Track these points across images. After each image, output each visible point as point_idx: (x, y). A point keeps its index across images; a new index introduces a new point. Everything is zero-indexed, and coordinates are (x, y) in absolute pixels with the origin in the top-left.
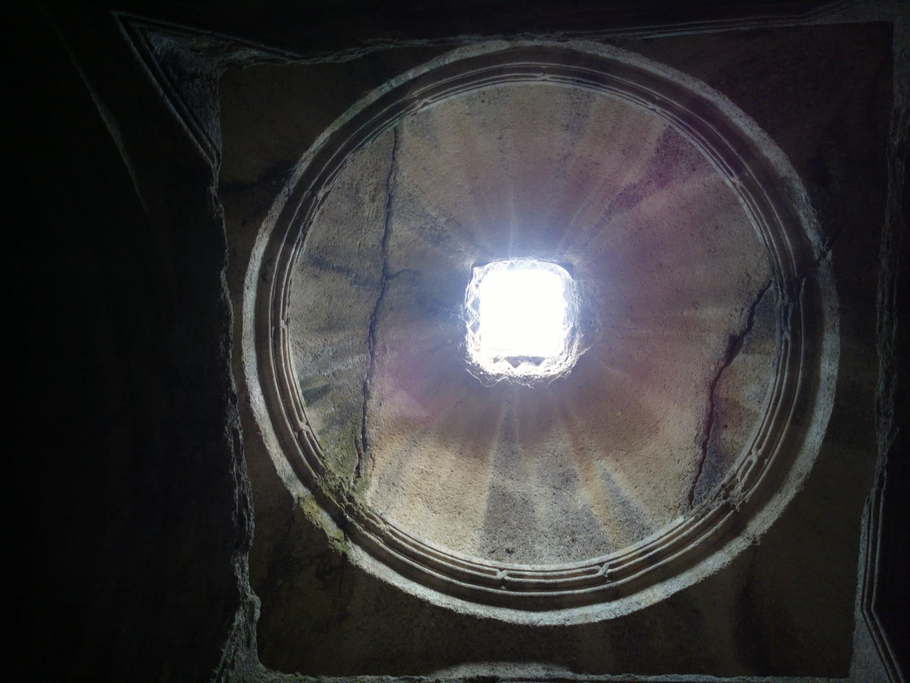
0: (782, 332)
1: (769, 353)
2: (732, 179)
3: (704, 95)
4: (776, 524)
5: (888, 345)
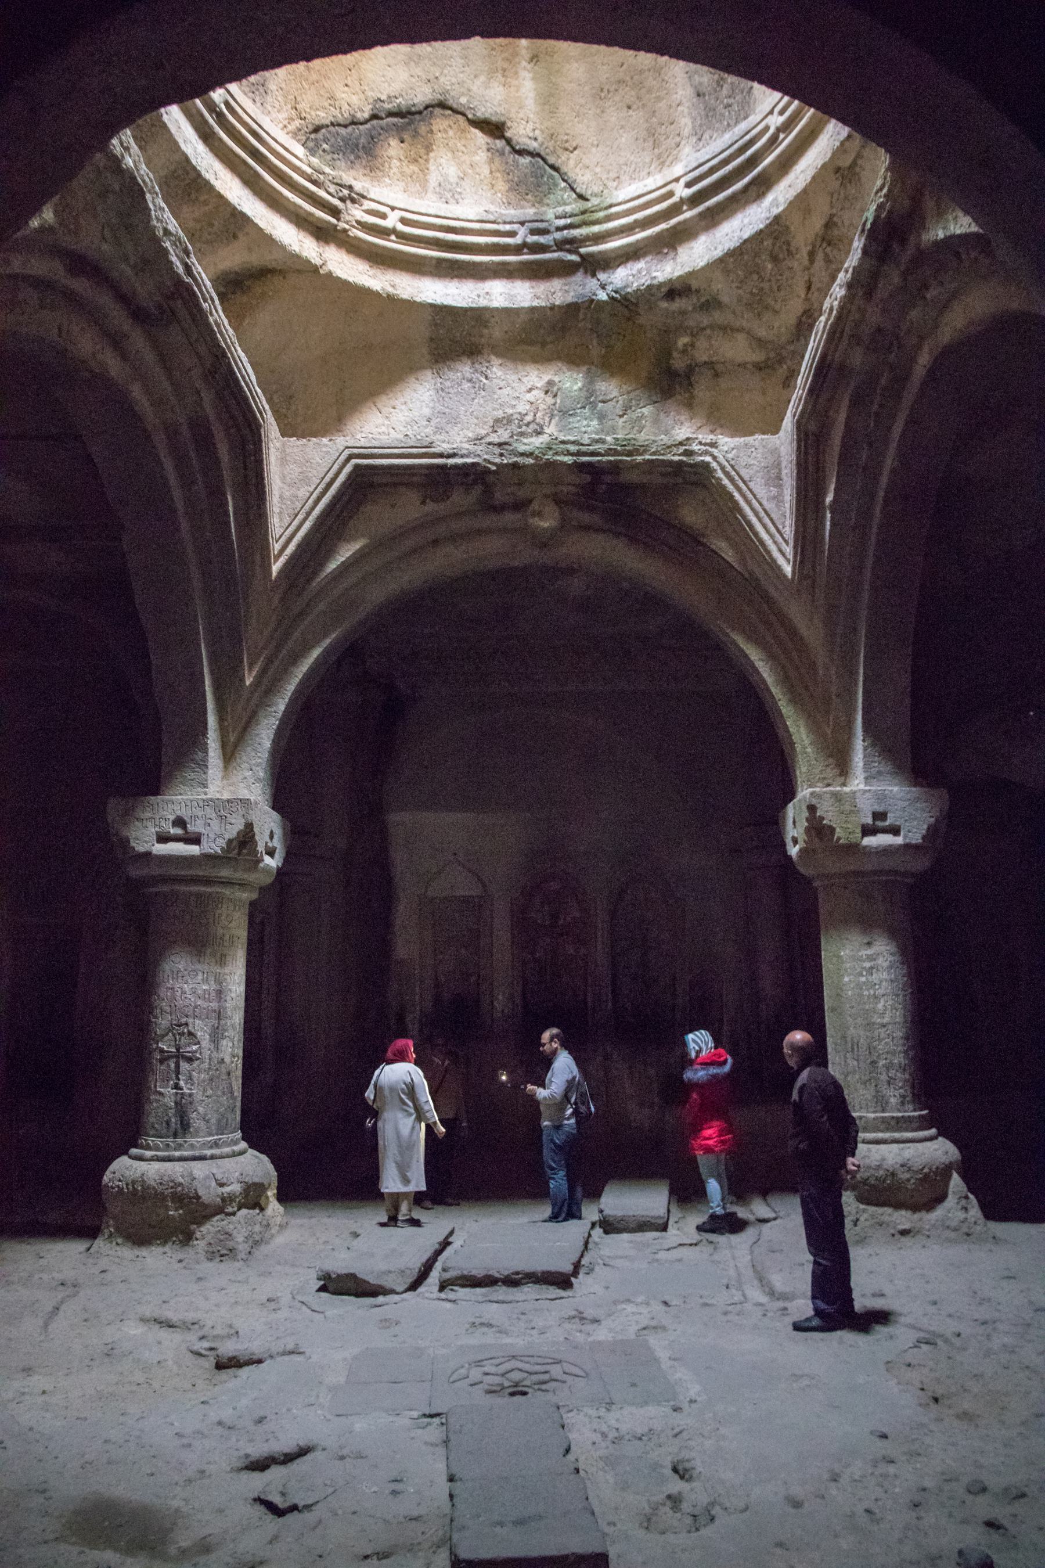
0: (522, 223)
1: (493, 186)
2: (682, 181)
3: (770, 197)
4: (346, 283)
5: (551, 453)
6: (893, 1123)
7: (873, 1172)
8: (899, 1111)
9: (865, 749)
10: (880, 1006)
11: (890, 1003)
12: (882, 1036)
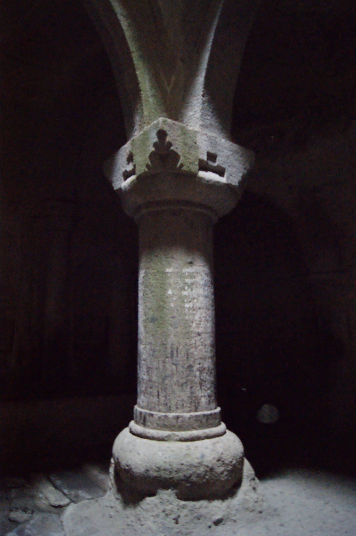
6: (204, 421)
7: (194, 469)
8: (207, 409)
9: (203, 103)
10: (197, 317)
11: (204, 315)
12: (198, 343)
